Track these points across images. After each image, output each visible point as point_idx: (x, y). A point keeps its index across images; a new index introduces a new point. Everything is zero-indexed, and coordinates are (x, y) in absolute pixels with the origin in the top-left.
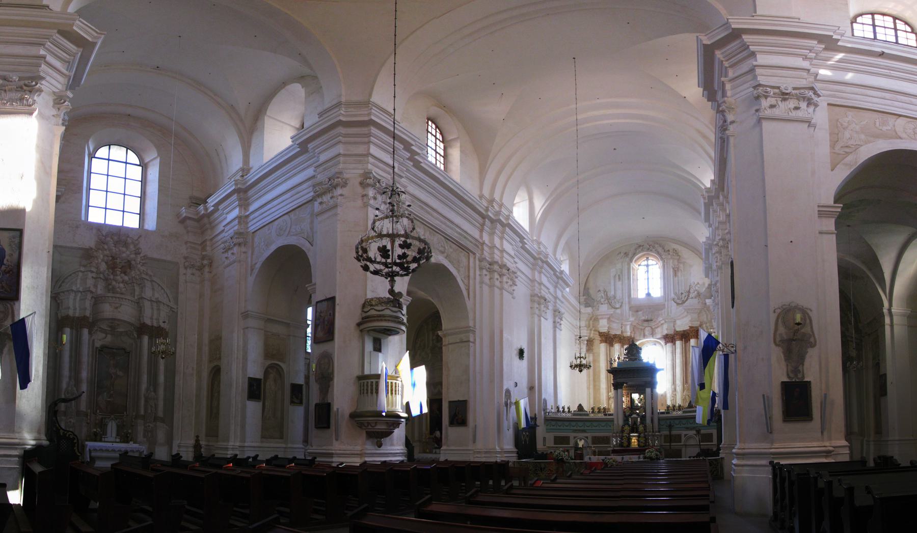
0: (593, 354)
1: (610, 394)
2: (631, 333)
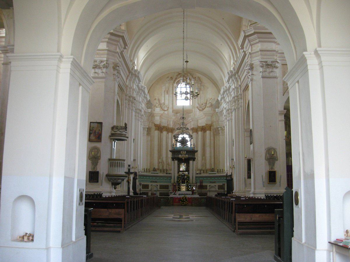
0: (151, 136)
2: (173, 126)
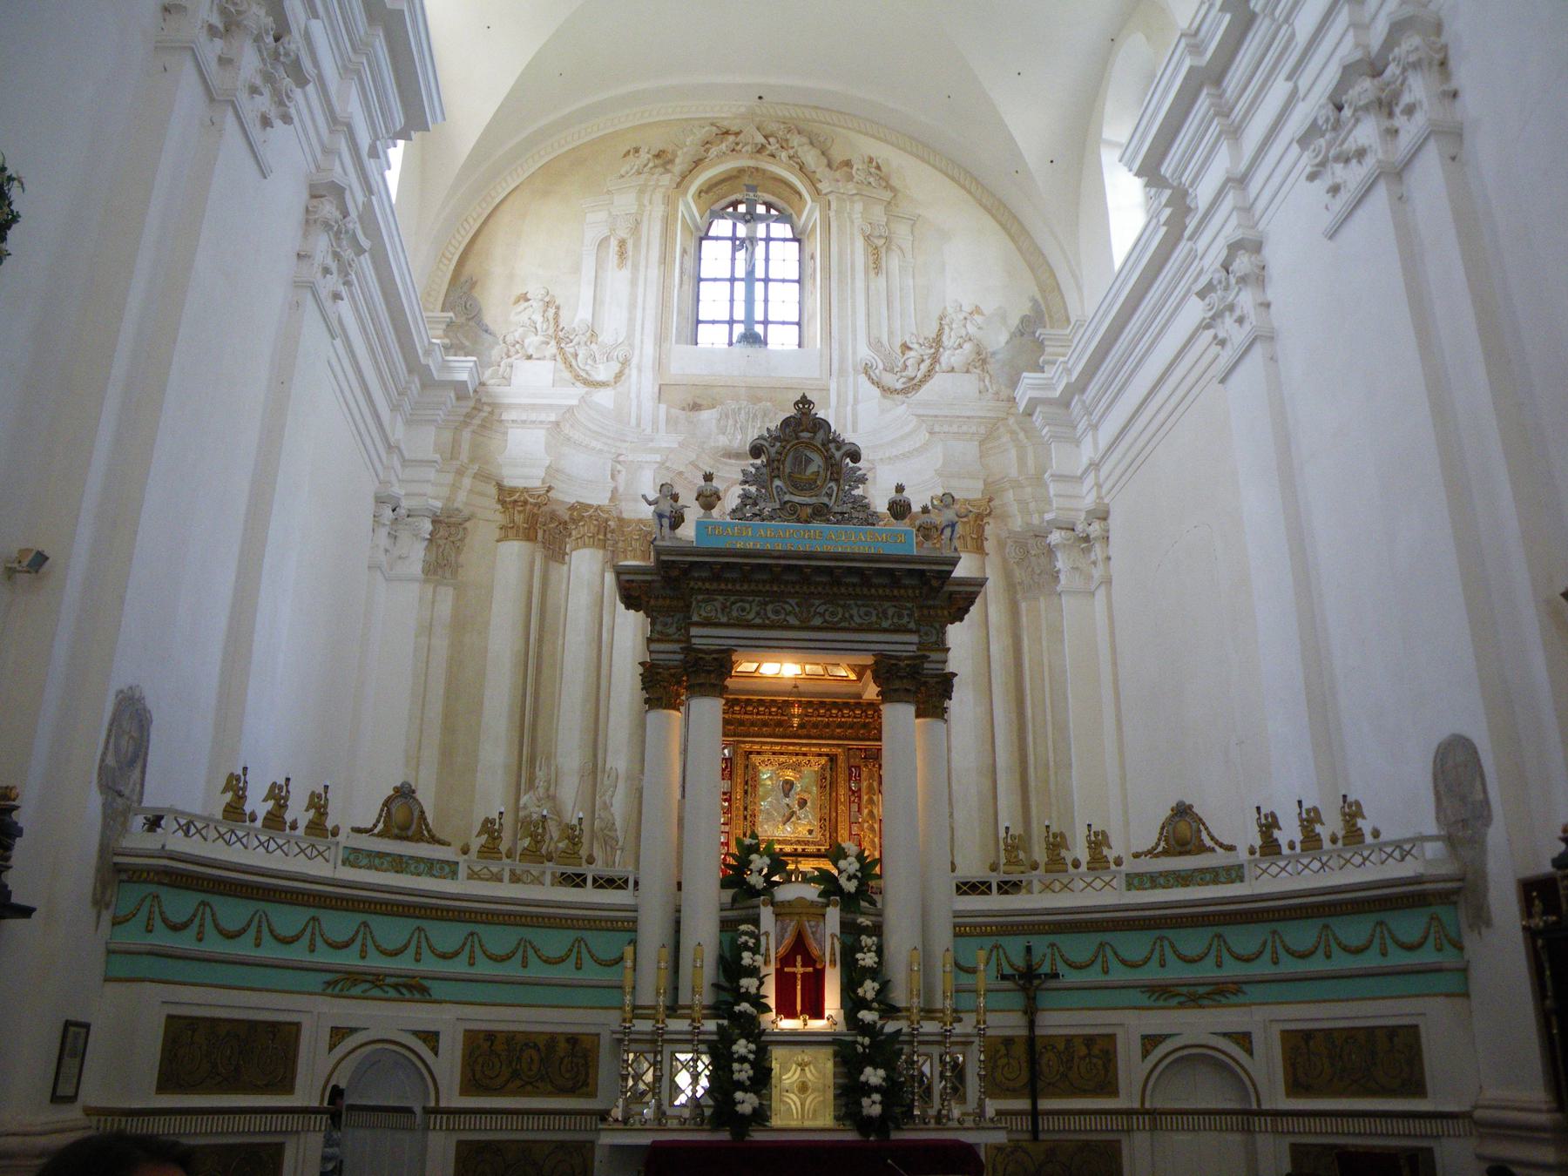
1: (524, 799)
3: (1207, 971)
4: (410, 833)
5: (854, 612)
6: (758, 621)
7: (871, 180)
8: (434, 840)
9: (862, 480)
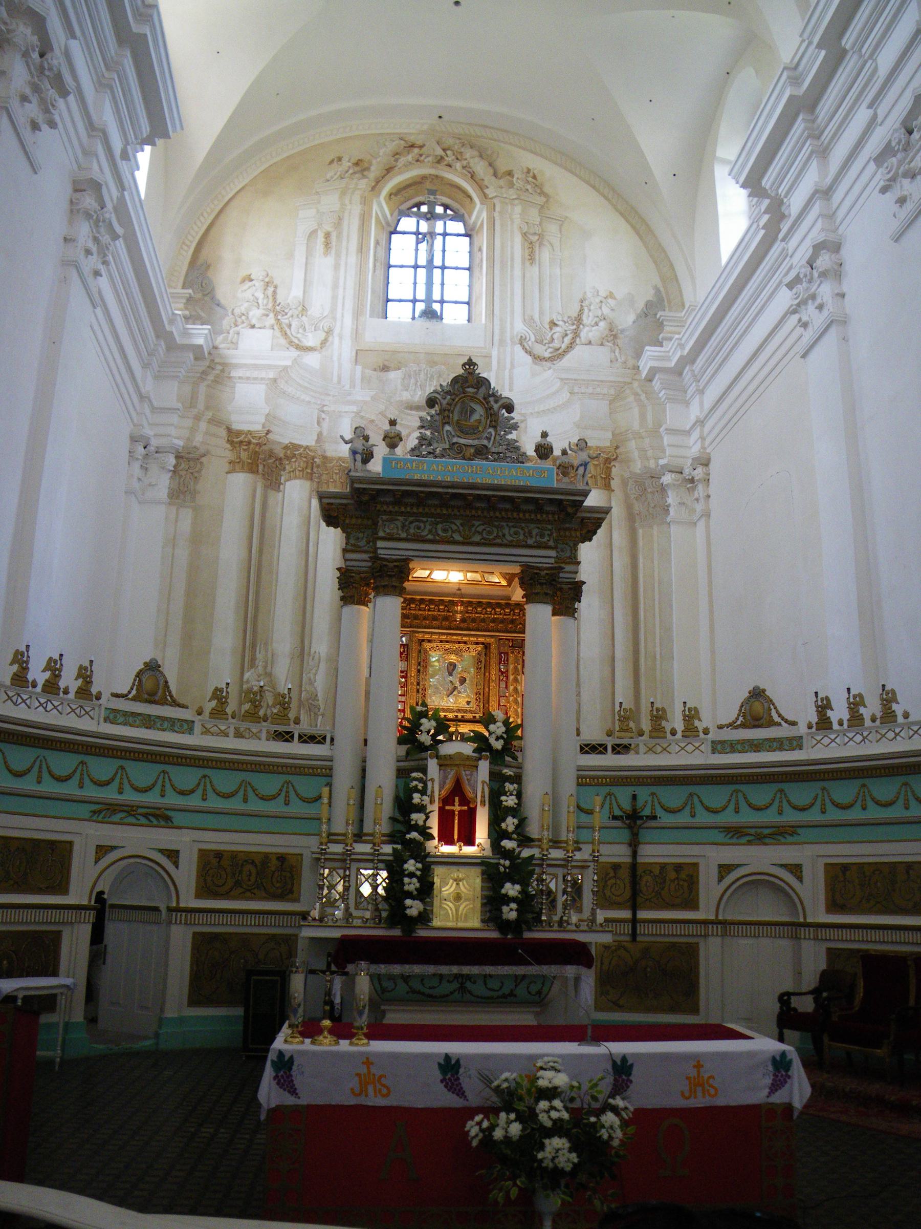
1: (247, 675)
3: (770, 817)
4: (157, 698)
5: (506, 531)
6: (430, 537)
7: (529, 187)
8: (175, 704)
9: (515, 427)
